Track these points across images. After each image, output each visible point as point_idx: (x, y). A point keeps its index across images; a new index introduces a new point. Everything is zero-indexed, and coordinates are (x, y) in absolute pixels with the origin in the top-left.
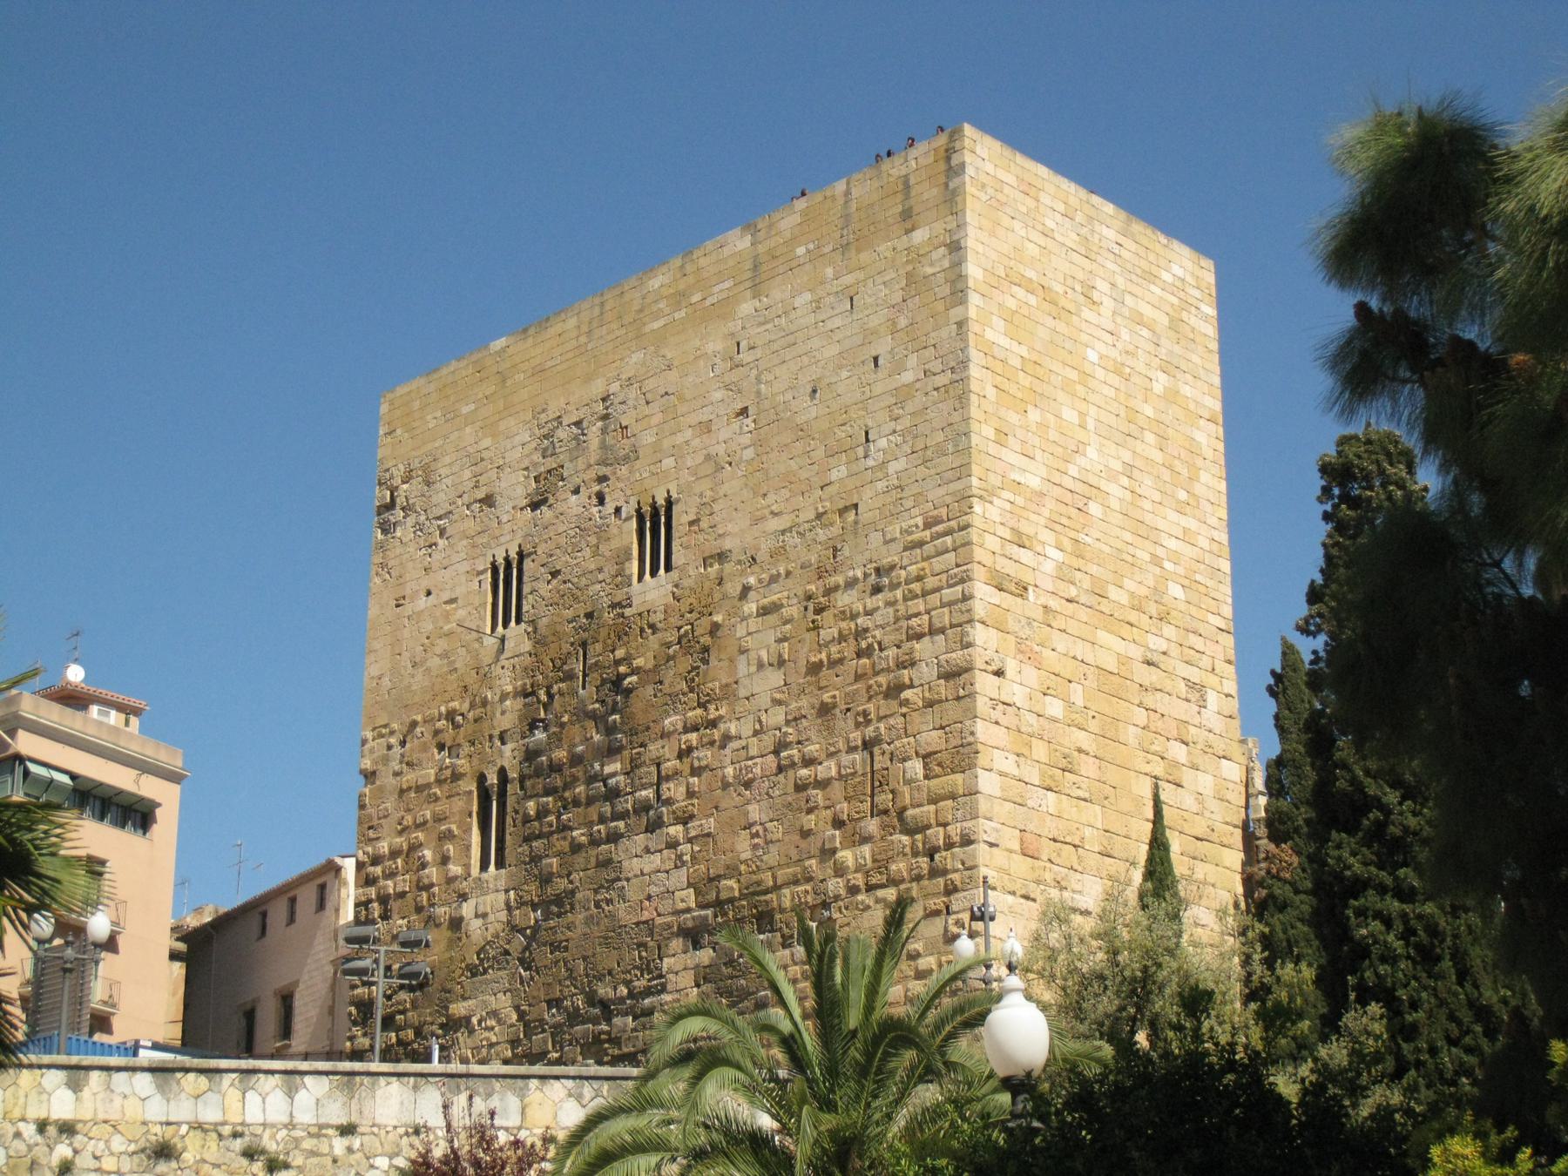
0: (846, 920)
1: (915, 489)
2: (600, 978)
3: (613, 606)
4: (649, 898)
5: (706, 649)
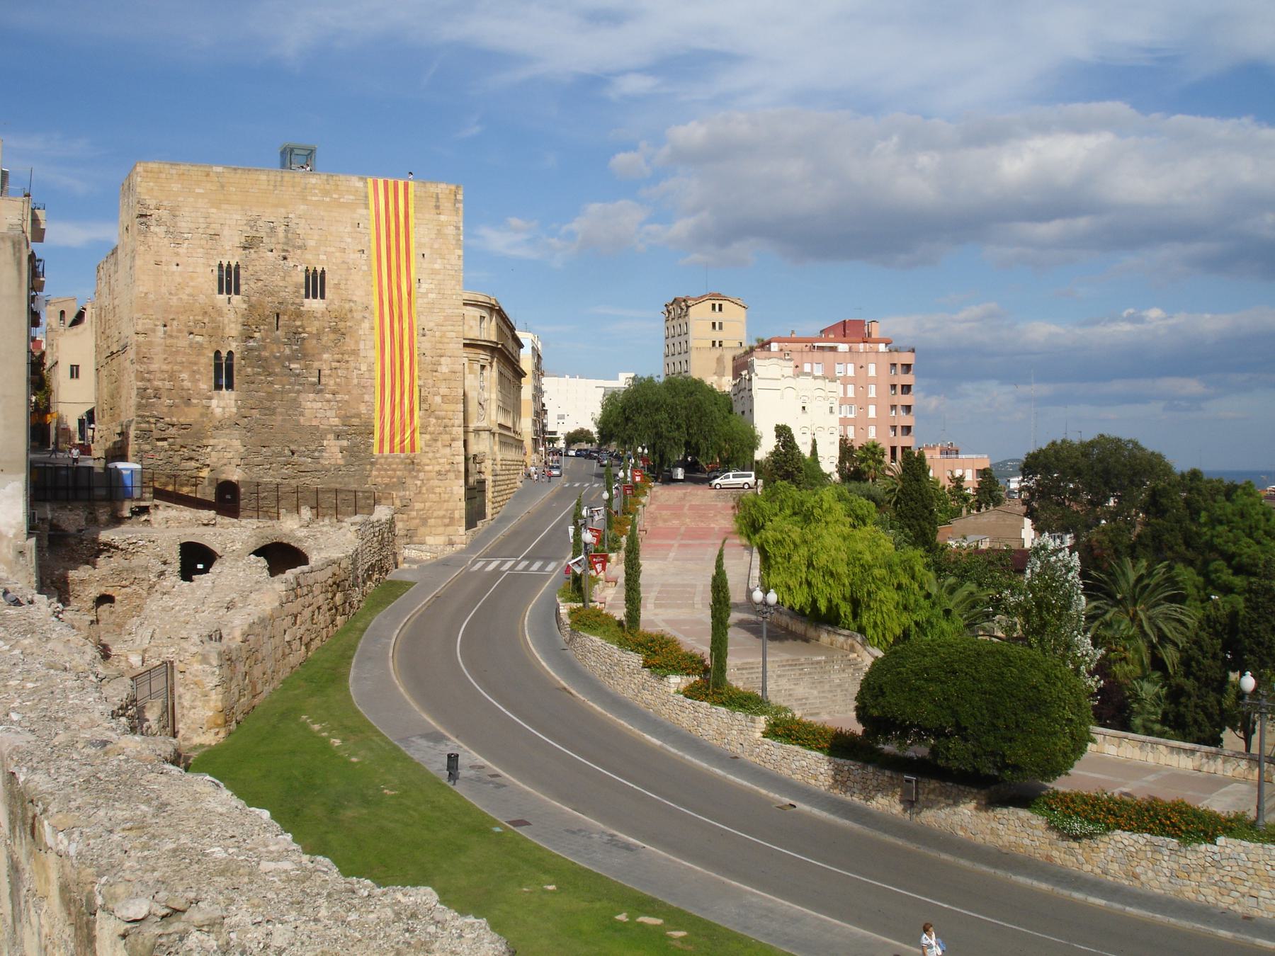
2: (291, 442)
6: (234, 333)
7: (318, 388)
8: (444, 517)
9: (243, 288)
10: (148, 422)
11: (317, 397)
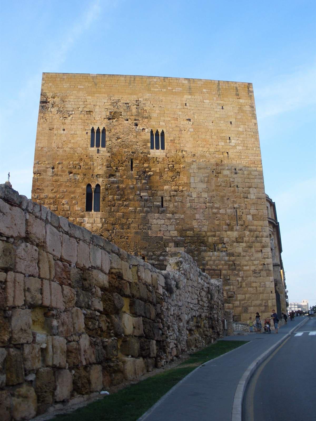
0: (231, 248)
1: (245, 154)
3: (142, 153)
4: (160, 230)
6: (101, 172)
8: (260, 305)
9: (107, 143)
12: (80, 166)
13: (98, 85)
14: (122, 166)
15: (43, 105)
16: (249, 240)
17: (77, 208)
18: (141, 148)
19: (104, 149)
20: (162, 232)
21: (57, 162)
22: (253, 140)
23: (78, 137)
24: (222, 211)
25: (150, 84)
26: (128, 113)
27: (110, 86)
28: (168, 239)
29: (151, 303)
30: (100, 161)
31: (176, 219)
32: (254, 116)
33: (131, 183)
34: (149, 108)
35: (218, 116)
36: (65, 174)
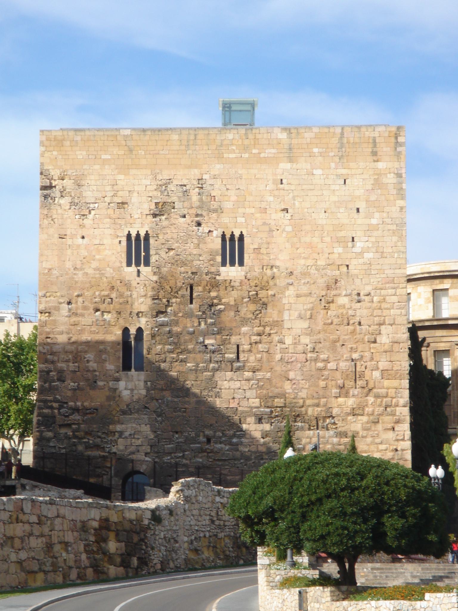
0: (343, 425)
1: (379, 267)
4: (234, 398)
5: (265, 304)
6: (144, 308)
7: (236, 365)
9: (153, 259)
10: (52, 408)
11: (235, 375)
12: (112, 299)
13: (134, 152)
14: (177, 297)
15: (46, 192)
16: (373, 411)
17: (110, 367)
18: (205, 265)
19: (148, 269)
20: (237, 401)
21: (76, 294)
22: (395, 239)
23: (105, 249)
24: (332, 365)
25: (221, 145)
26: (186, 204)
27: (154, 152)
28: (246, 411)
29: (134, 532)
30: (142, 290)
31: (258, 380)
32: (402, 192)
33: (190, 325)
34: (220, 192)
35: (335, 199)
36: (89, 312)
